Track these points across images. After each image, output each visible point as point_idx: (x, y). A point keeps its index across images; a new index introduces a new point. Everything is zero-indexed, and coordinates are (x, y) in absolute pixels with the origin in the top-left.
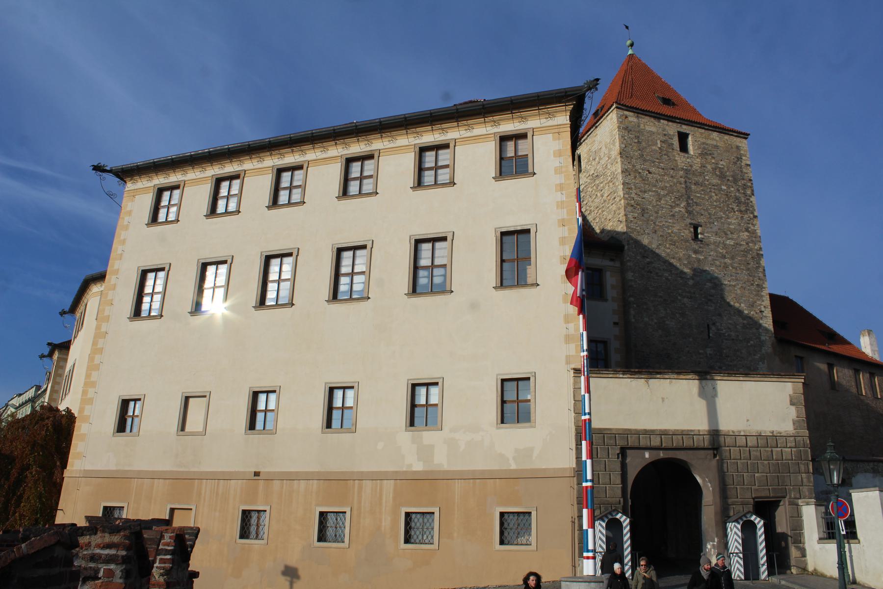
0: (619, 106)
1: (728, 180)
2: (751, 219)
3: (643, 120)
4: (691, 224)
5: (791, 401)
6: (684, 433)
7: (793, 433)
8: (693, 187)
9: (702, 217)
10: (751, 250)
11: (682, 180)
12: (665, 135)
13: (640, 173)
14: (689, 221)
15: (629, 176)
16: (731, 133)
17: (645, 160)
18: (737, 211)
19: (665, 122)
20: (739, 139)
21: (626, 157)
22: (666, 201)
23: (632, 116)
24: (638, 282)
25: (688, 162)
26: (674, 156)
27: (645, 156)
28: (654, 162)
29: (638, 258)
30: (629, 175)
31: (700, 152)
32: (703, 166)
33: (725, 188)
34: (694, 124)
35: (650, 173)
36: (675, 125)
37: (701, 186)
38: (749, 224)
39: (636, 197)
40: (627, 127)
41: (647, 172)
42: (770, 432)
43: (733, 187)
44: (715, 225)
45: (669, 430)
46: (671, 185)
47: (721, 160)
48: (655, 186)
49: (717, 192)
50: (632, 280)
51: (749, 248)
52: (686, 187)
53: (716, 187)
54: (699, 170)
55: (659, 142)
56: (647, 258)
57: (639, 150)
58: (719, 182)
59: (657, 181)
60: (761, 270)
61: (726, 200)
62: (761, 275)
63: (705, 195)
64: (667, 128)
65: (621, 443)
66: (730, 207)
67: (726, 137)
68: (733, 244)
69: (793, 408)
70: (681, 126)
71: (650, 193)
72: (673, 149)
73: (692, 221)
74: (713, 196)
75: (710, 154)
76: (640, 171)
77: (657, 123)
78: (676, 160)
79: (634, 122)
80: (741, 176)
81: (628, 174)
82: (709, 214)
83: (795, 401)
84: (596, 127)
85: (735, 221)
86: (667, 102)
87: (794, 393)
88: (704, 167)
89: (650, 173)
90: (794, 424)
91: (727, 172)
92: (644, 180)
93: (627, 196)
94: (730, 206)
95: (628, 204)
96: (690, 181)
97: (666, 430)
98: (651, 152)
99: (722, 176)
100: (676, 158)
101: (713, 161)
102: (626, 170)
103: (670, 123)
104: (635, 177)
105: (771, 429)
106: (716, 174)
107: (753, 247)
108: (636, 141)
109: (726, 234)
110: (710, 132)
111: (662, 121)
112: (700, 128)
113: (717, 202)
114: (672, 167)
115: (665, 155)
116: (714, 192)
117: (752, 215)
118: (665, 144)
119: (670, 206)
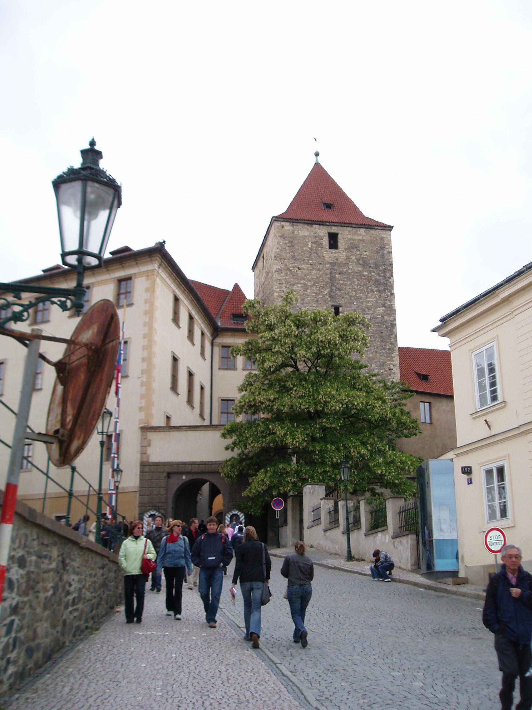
0: (276, 219)
1: (370, 267)
2: (388, 296)
3: (297, 227)
4: (332, 306)
8: (337, 276)
9: (343, 299)
10: (386, 321)
11: (328, 272)
12: (316, 237)
13: (291, 270)
14: (330, 303)
15: (281, 274)
16: (376, 228)
17: (296, 260)
18: (376, 291)
19: (317, 226)
20: (384, 232)
21: (281, 259)
22: (312, 290)
23: (287, 226)
25: (335, 257)
26: (323, 253)
27: (296, 256)
28: (304, 260)
30: (282, 273)
31: (346, 247)
32: (348, 258)
33: (367, 273)
34: (342, 225)
35: (299, 269)
36: (326, 227)
37: (345, 274)
38: (385, 300)
39: (285, 290)
40: (283, 235)
41: (297, 269)
43: (374, 272)
44: (354, 305)
45: (197, 462)
46: (317, 277)
47: (366, 251)
48: (304, 279)
49: (359, 277)
51: (383, 320)
52: (331, 277)
53: (358, 274)
54: (344, 262)
55: (310, 243)
57: (292, 252)
58: (361, 269)
59: (305, 275)
60: (393, 336)
61: (367, 284)
62: (393, 340)
63: (347, 281)
64: (318, 231)
65: (168, 469)
66: (369, 289)
67: (372, 231)
68: (369, 318)
70: (331, 228)
71: (298, 285)
72: (322, 248)
73: (334, 304)
74: (355, 282)
75: (356, 247)
76: (291, 269)
77: (309, 228)
78: (324, 257)
79: (289, 230)
80: (382, 262)
81: (280, 272)
82: (350, 296)
84: (268, 234)
85: (373, 300)
86: (328, 206)
88: (349, 258)
89: (299, 269)
91: (369, 260)
92: (293, 275)
93: (278, 290)
94: (370, 288)
95: (278, 296)
96: (335, 272)
98: (302, 252)
99: (365, 264)
100: (324, 255)
101: (358, 253)
102: (279, 269)
103: (321, 227)
104: (286, 274)
106: (359, 263)
107: (388, 319)
108: (290, 245)
109: (364, 310)
110: (358, 229)
111: (314, 226)
112: (348, 227)
113: (357, 286)
114: (320, 262)
115: (314, 253)
116: (356, 278)
117: (389, 293)
118: (315, 244)
119: (315, 293)
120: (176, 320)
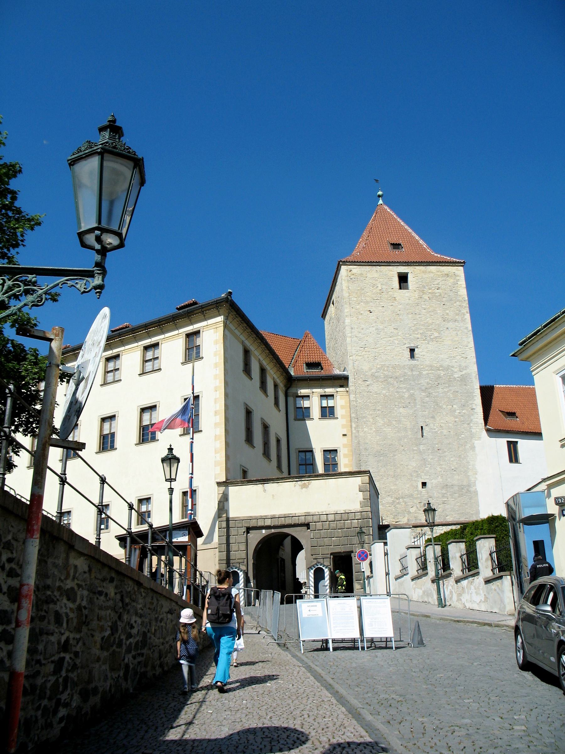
4: (407, 348)
24: (359, 401)
83: (362, 489)
105: (344, 509)
120: (247, 370)
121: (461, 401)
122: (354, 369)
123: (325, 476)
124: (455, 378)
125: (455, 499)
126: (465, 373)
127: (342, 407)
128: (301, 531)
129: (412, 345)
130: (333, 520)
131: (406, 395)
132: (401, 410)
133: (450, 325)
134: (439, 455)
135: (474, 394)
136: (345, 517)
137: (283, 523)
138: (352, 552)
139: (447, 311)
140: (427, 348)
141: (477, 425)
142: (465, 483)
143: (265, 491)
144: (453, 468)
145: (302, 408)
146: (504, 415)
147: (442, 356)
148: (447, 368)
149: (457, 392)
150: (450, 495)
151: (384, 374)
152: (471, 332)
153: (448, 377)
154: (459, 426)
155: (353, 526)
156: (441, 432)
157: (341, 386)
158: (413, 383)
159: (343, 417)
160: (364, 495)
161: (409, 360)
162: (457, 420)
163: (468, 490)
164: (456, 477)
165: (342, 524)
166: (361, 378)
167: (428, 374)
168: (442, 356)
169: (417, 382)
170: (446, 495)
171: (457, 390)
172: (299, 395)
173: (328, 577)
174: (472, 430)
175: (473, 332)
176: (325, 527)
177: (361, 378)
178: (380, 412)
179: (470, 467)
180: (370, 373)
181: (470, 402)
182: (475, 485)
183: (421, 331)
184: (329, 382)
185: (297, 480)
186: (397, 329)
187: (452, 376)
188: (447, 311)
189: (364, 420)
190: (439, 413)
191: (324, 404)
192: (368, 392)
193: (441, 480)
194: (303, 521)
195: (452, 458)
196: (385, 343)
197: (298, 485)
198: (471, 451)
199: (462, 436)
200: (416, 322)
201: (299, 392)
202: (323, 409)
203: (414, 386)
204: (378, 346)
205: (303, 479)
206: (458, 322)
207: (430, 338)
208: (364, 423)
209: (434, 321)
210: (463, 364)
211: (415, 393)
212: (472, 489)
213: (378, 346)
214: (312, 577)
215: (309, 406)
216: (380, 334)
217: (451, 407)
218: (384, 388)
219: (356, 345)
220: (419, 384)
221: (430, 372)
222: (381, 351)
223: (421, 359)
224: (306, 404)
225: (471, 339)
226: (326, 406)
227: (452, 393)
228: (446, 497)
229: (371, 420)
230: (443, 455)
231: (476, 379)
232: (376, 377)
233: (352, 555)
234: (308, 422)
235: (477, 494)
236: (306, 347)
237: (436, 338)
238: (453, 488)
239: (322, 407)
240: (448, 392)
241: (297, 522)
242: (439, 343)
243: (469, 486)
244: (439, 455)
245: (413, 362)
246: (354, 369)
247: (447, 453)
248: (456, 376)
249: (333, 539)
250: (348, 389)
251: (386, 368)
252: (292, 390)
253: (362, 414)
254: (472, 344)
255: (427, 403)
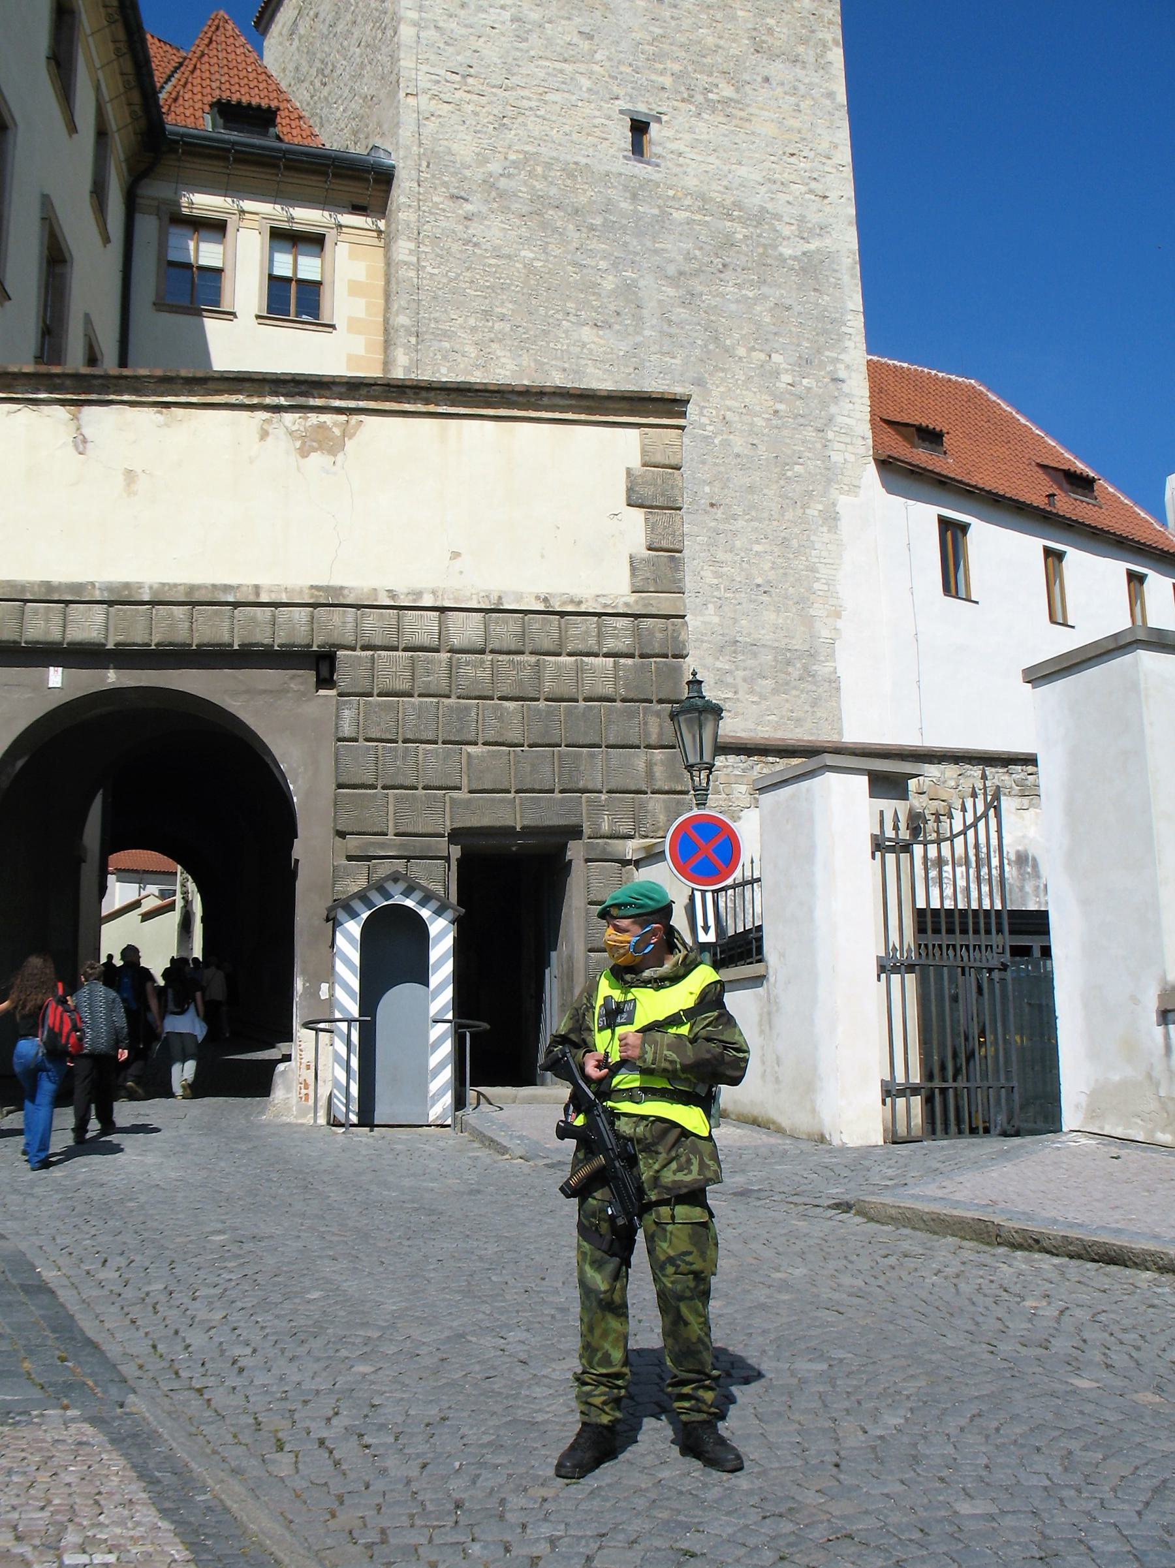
4: (622, 112)
5: (630, 490)
6: (197, 597)
7: (627, 604)
24: (429, 269)
29: (436, 199)
42: (538, 598)
45: (140, 586)
50: (406, 263)
56: (466, 200)
69: (638, 515)
83: (647, 492)
87: (644, 465)
90: (633, 569)
97: (127, 586)
105: (543, 590)
121: (799, 345)
122: (420, 144)
123: (442, 396)
124: (782, 259)
125: (763, 697)
126: (818, 250)
127: (356, 289)
128: (281, 692)
129: (642, 108)
130: (479, 642)
131: (609, 283)
132: (587, 333)
133: (777, 69)
134: (713, 524)
135: (844, 329)
136: (544, 632)
137: (181, 635)
138: (575, 832)
139: (771, 22)
140: (691, 130)
141: (848, 440)
142: (797, 644)
143: (81, 443)
144: (759, 581)
145: (188, 266)
146: (906, 438)
147: (743, 171)
148: (760, 217)
149: (788, 308)
150: (745, 680)
151: (533, 188)
152: (844, 113)
153: (761, 250)
154: (785, 432)
155: (587, 690)
156: (726, 444)
157: (358, 209)
158: (634, 243)
159: (354, 325)
160: (651, 528)
161: (625, 157)
162: (781, 407)
163: (806, 668)
164: (770, 616)
165: (527, 672)
166: (445, 184)
167: (690, 222)
168: (743, 171)
169: (649, 244)
170: (729, 679)
171: (788, 302)
172: (185, 211)
173: (448, 968)
174: (832, 453)
175: (850, 112)
176: (422, 680)
177: (445, 184)
178: (507, 327)
179: (816, 586)
180: (479, 174)
181: (827, 353)
182: (831, 656)
183: (677, 67)
184: (313, 180)
185: (282, 401)
186: (591, 38)
187: (775, 247)
188: (771, 22)
189: (446, 345)
190: (723, 370)
191: (283, 265)
192: (467, 242)
193: (716, 620)
194: (300, 637)
195: (757, 542)
196: (542, 75)
197: (281, 432)
198: (825, 529)
199: (797, 467)
200: (659, 31)
201: (184, 201)
202: (277, 286)
203: (638, 254)
204: (515, 80)
205: (312, 402)
206: (804, 68)
207: (707, 100)
208: (444, 358)
209: (722, 42)
210: (813, 218)
211: (641, 283)
212: (823, 670)
213: (515, 80)
214: (347, 962)
215: (218, 264)
216: (526, 40)
217: (763, 356)
218: (525, 241)
219: (433, 57)
220: (656, 252)
221: (698, 217)
222: (526, 103)
223: (670, 165)
224: (208, 254)
225: (843, 135)
226: (289, 274)
227: (771, 310)
228: (728, 685)
229: (472, 351)
230: (727, 527)
231: (853, 276)
232: (502, 195)
233: (575, 851)
234: (212, 326)
235: (838, 689)
236: (214, 60)
237: (726, 102)
238: (755, 655)
239: (273, 279)
240: (756, 299)
241: (262, 637)
242: (735, 122)
243: (812, 655)
244: (713, 524)
245: (639, 169)
246: (420, 144)
247: (741, 523)
248: (787, 251)
249: (470, 749)
250: (382, 224)
251: (539, 170)
252: (154, 190)
253: (436, 321)
254: (844, 155)
255: (680, 325)
